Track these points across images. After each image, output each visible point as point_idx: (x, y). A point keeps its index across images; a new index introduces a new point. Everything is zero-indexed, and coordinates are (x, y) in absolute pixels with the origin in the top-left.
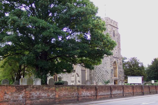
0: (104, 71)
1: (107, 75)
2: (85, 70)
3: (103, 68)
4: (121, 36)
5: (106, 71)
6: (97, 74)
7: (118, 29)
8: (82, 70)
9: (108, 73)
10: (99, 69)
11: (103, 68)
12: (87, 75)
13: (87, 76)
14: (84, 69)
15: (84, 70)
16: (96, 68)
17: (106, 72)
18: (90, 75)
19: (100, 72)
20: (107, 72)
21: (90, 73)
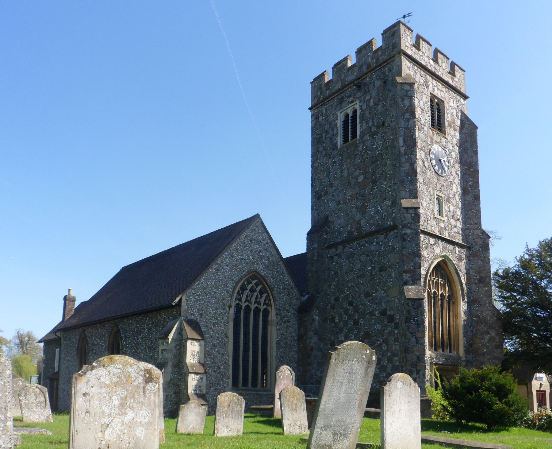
0: (371, 314)
1: (391, 333)
2: (266, 313)
3: (368, 295)
4: (479, 131)
5: (383, 313)
6: (341, 331)
7: (465, 97)
8: (238, 307)
9: (396, 327)
10: (351, 304)
11: (368, 295)
12: (275, 340)
13: (274, 346)
14: (253, 307)
15: (257, 310)
16: (337, 299)
17: (386, 321)
18: (301, 338)
19: (356, 323)
20: (391, 319)
21: (300, 325)
